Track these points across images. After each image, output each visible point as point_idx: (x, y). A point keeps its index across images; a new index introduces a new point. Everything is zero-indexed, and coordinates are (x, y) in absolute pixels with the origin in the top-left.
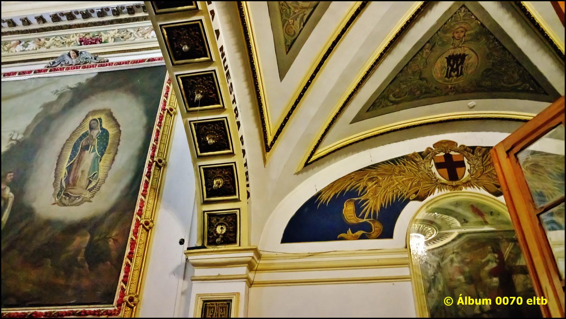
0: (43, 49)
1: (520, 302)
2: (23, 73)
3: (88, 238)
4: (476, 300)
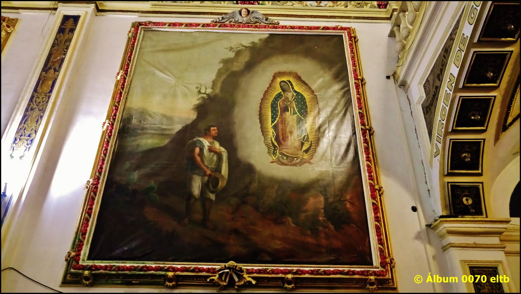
1: (484, 280)
2: (174, 25)
3: (322, 199)
4: (444, 278)
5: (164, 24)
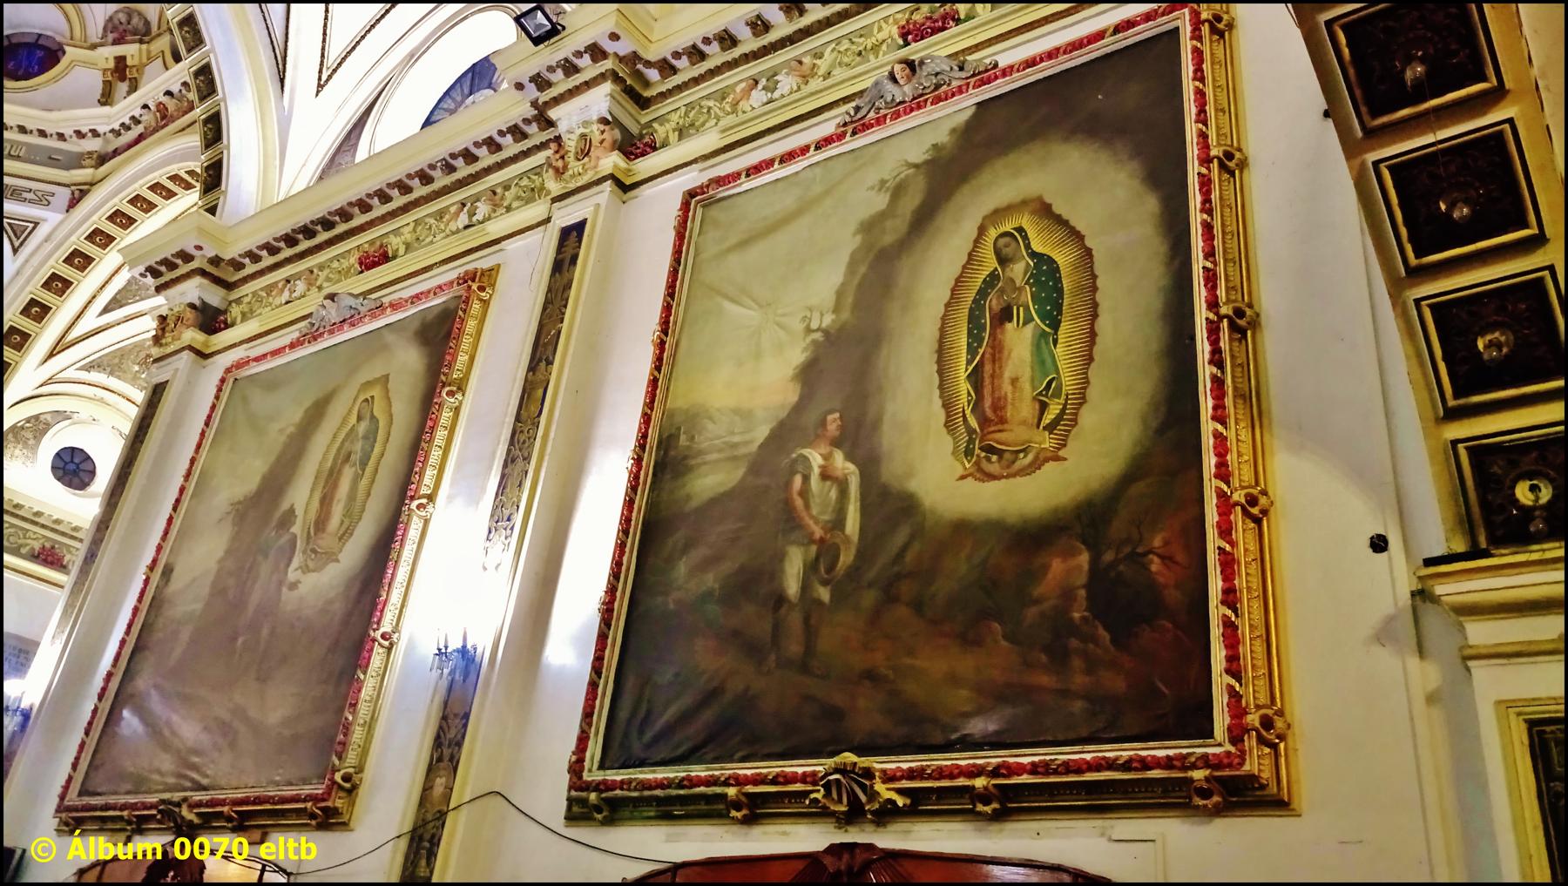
0: (815, 84)
3: (1084, 559)
5: (735, 176)
